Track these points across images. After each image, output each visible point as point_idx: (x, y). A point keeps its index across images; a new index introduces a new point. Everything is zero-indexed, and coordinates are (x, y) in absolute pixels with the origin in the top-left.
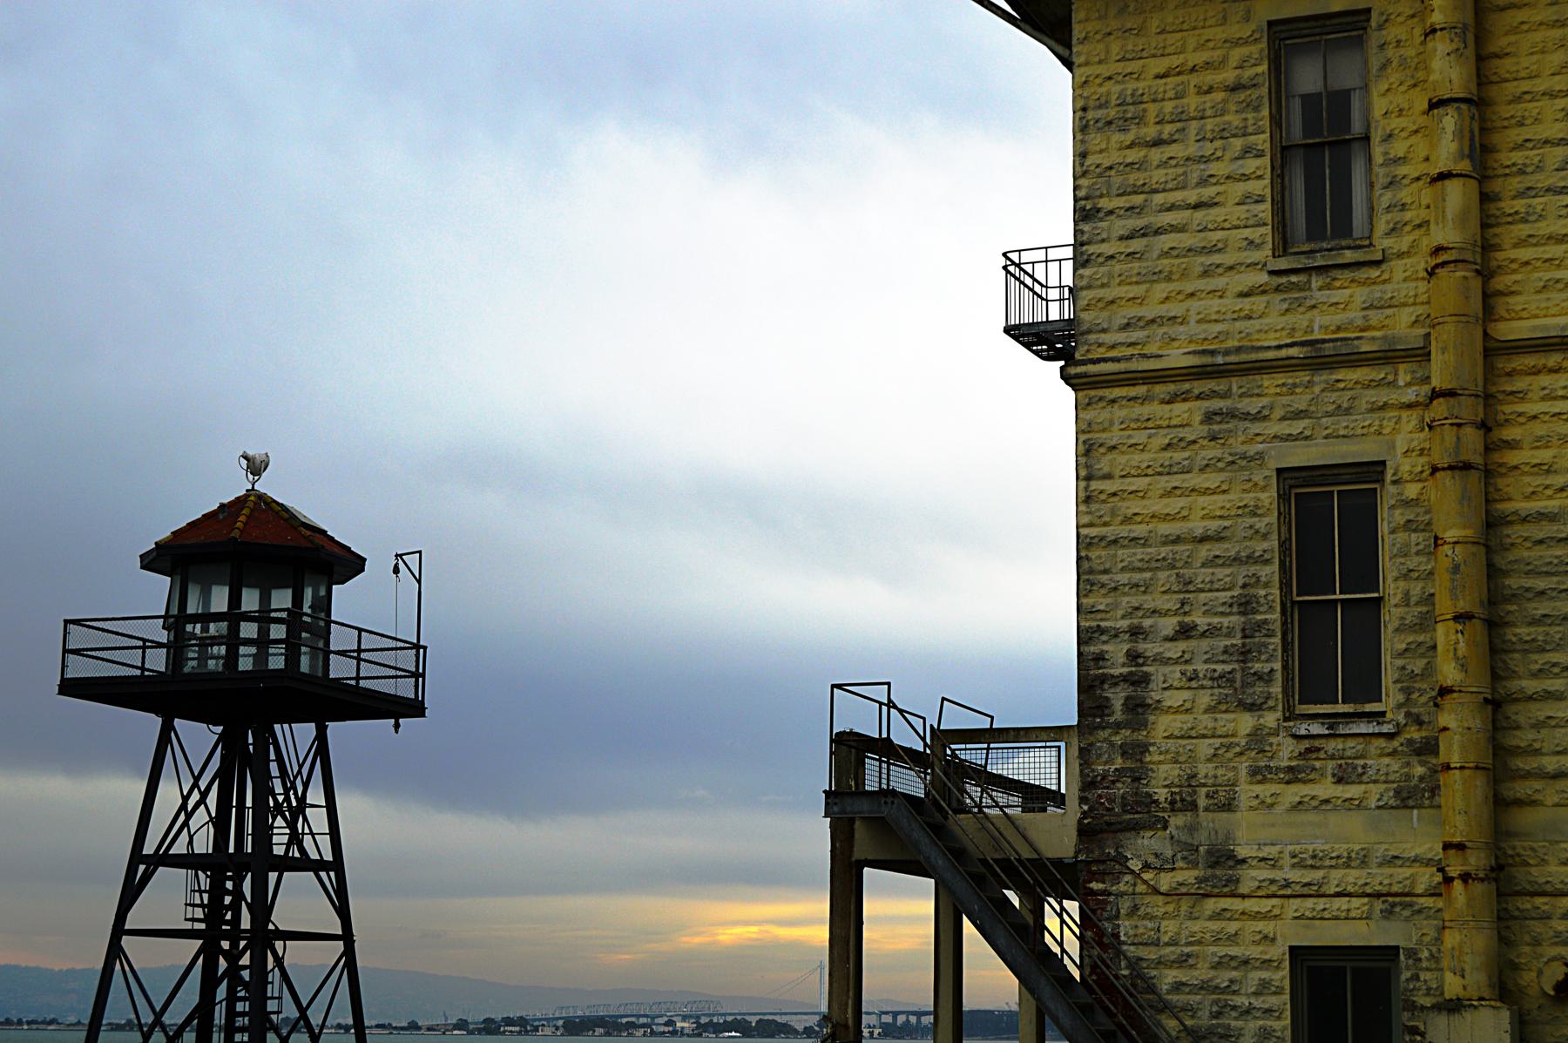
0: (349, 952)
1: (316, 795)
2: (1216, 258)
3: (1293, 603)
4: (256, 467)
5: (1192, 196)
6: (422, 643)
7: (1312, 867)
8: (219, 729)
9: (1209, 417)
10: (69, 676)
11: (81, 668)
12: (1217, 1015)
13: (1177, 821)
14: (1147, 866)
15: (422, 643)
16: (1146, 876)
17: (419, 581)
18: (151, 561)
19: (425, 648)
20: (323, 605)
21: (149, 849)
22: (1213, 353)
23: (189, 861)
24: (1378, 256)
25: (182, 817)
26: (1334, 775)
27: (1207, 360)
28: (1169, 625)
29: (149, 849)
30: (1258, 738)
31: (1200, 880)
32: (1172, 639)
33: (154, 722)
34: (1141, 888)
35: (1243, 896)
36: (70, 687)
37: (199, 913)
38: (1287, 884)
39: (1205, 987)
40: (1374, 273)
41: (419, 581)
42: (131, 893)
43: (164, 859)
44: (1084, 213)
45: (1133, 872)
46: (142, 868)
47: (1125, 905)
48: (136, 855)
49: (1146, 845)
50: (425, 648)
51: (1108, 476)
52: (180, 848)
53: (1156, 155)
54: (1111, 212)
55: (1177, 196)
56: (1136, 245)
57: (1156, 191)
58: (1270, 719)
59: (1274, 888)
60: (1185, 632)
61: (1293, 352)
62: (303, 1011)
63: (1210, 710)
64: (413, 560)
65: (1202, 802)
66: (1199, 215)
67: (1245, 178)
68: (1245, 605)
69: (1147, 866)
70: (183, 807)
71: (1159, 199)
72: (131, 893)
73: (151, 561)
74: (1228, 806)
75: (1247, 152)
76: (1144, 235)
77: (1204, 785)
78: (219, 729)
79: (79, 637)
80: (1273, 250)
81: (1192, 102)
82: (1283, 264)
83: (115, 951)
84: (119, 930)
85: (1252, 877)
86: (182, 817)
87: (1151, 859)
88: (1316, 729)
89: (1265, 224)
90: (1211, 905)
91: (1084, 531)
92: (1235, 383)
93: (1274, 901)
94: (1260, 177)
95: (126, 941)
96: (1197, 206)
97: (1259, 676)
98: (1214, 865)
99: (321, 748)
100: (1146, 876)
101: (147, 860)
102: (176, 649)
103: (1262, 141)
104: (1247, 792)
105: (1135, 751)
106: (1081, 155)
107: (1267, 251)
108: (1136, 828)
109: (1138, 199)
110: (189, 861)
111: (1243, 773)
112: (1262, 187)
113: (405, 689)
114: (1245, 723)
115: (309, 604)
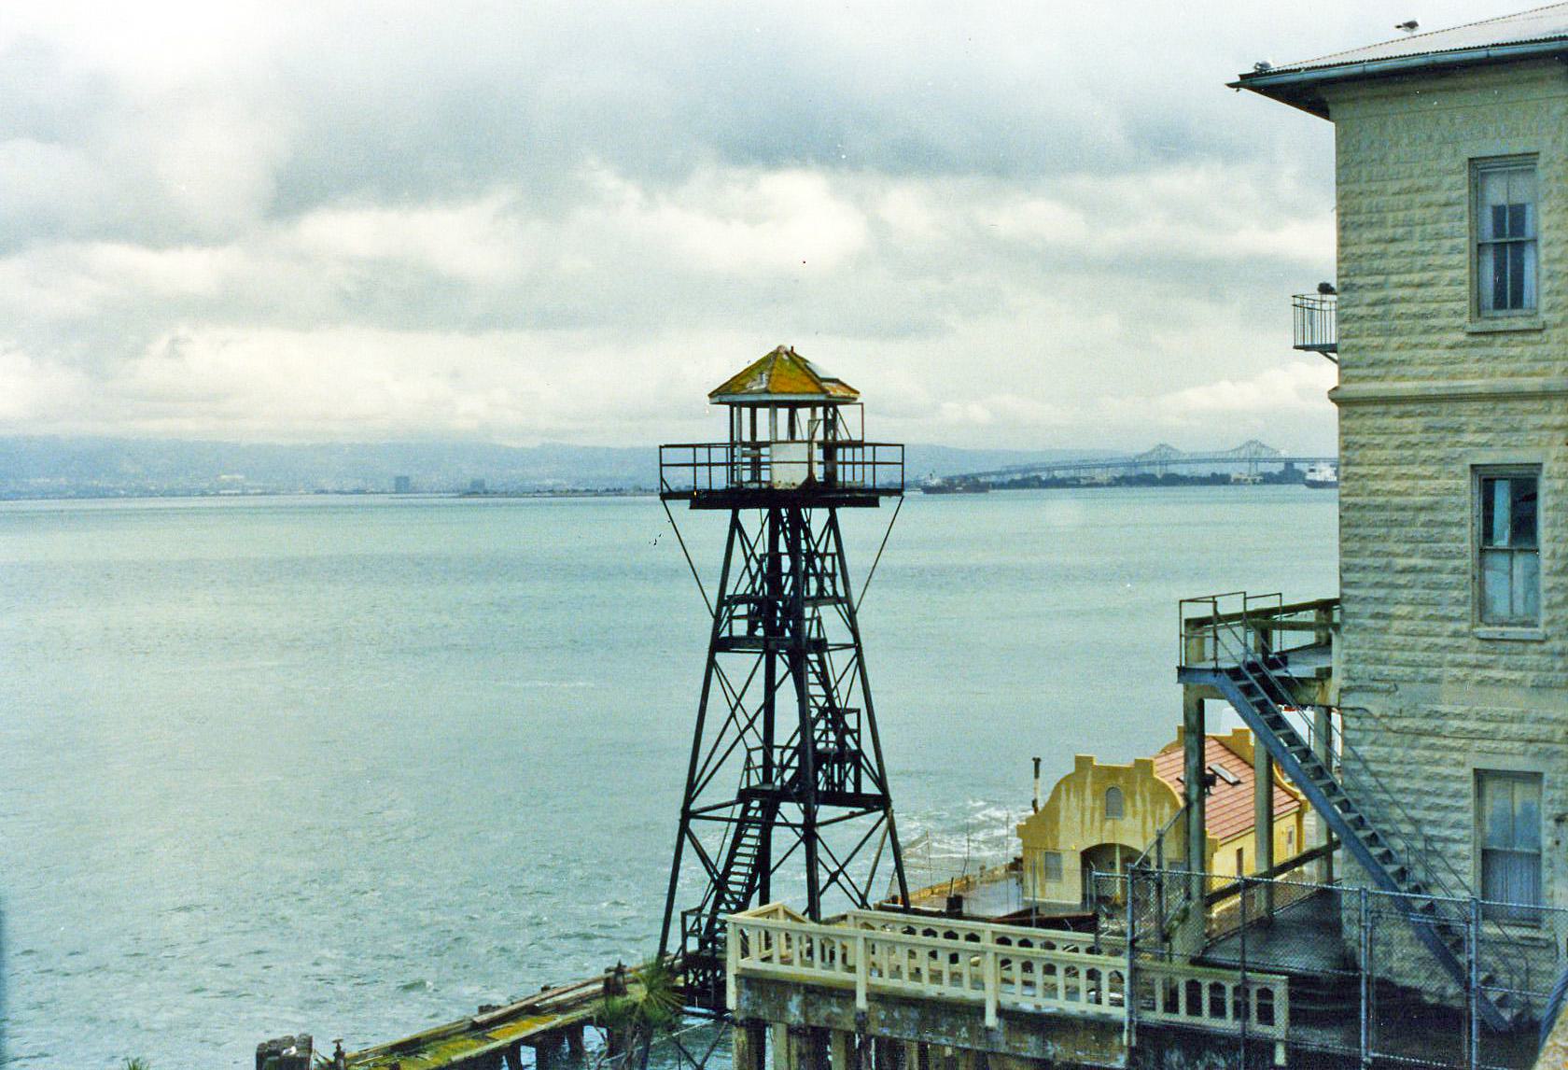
2: (1433, 322)
5: (1416, 278)
24: (1540, 326)
40: (1536, 337)
53: (1393, 248)
55: (1408, 278)
56: (1378, 310)
57: (1392, 273)
66: (1421, 292)
67: (1451, 267)
71: (1394, 279)
76: (1384, 304)
81: (1417, 214)
82: (1476, 328)
89: (1464, 300)
94: (1462, 267)
96: (1420, 285)
103: (1463, 242)
107: (1466, 318)
109: (1379, 279)
112: (1463, 274)
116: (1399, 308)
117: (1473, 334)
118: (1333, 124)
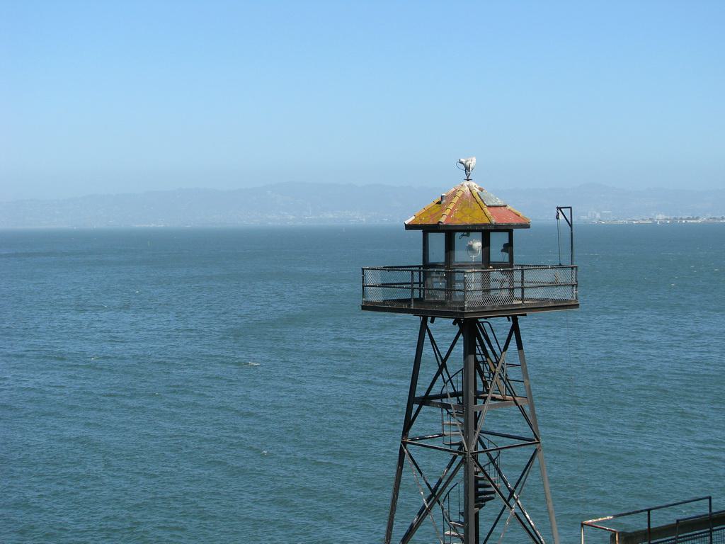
11: (376, 296)
19: (576, 267)
20: (508, 247)
29: (420, 393)
33: (417, 320)
43: (426, 400)
48: (412, 399)
64: (566, 212)
99: (515, 329)
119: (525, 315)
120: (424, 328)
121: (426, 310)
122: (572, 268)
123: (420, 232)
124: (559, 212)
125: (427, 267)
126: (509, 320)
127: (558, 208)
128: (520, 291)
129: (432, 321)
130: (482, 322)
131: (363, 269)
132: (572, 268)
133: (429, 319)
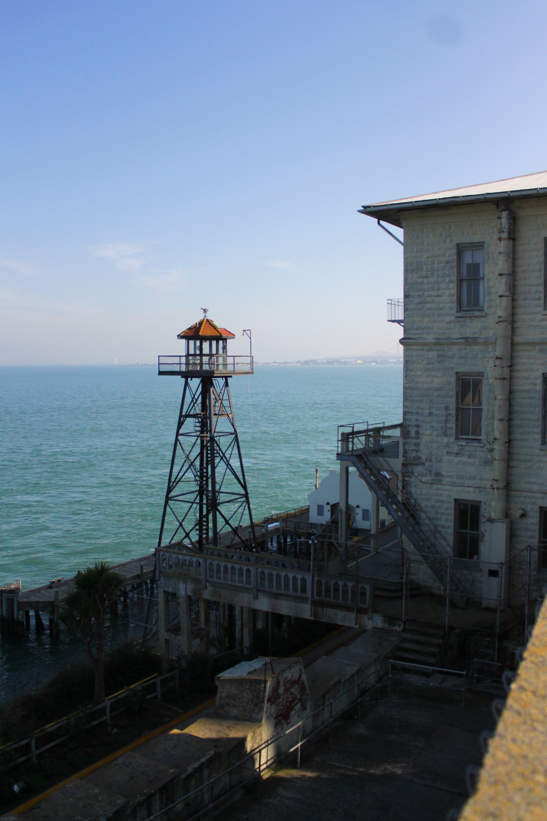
0: (236, 437)
1: (226, 397)
3: (459, 408)
4: (205, 311)
5: (435, 293)
6: (252, 355)
7: (461, 479)
8: (201, 379)
9: (439, 356)
10: (161, 370)
11: (164, 368)
12: (436, 514)
13: (427, 464)
14: (419, 475)
15: (252, 355)
16: (419, 477)
17: (250, 338)
18: (180, 337)
20: (224, 348)
21: (184, 413)
22: (440, 339)
23: (195, 416)
24: (484, 314)
25: (192, 403)
26: (467, 456)
27: (438, 341)
28: (427, 412)
29: (184, 413)
30: (448, 445)
31: (432, 480)
32: (428, 416)
34: (418, 480)
35: (443, 485)
36: (161, 373)
37: (199, 429)
38: (454, 483)
39: (433, 506)
40: (483, 319)
41: (250, 338)
42: (180, 424)
43: (188, 416)
44: (406, 296)
45: (416, 476)
46: (182, 419)
47: (413, 484)
48: (181, 416)
49: (418, 470)
50: (253, 357)
51: (412, 370)
52: (192, 413)
53: (425, 281)
54: (413, 296)
55: (431, 293)
56: (420, 306)
57: (425, 291)
58: (452, 439)
59: (451, 484)
60: (430, 414)
61: (461, 340)
62: (224, 454)
63: (437, 436)
64: (248, 332)
65: (434, 460)
66: (437, 299)
67: (450, 289)
68: (447, 408)
69: (419, 475)
70: (192, 401)
71: (426, 293)
72: (180, 424)
73: (180, 337)
74: (440, 461)
75: (450, 281)
76: (422, 303)
77: (434, 455)
78: (201, 379)
79: (163, 360)
80: (457, 310)
81: (436, 266)
82: (459, 315)
83: (177, 440)
84: (178, 434)
85: (446, 480)
86: (192, 403)
87: (420, 474)
88: (463, 443)
89: (454, 303)
90: (435, 486)
91: (405, 385)
92: (446, 347)
93: (451, 487)
94: (453, 289)
95: (180, 438)
96: (437, 296)
97: (449, 428)
98: (436, 476)
99: (227, 384)
100: (419, 477)
101: (184, 416)
102: (187, 364)
103: (454, 278)
104: (446, 458)
105: (417, 444)
106: (406, 280)
107: (455, 310)
108: (416, 464)
109: (421, 293)
110: (195, 416)
111: (445, 453)
112: (454, 292)
113: (247, 368)
114: (446, 440)
115: (222, 347)
116: (429, 305)
117: (457, 317)
118: (402, 230)
119: (231, 377)
120: (186, 384)
121: (187, 375)
122: (251, 356)
123: (184, 341)
124: (244, 332)
125: (188, 355)
126: (223, 380)
127: (243, 330)
128: (232, 366)
129: (191, 380)
130: (215, 380)
131: (159, 356)
132: (251, 356)
133: (189, 379)
